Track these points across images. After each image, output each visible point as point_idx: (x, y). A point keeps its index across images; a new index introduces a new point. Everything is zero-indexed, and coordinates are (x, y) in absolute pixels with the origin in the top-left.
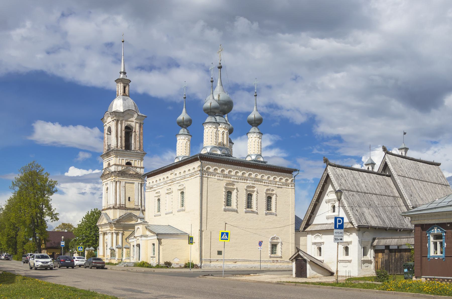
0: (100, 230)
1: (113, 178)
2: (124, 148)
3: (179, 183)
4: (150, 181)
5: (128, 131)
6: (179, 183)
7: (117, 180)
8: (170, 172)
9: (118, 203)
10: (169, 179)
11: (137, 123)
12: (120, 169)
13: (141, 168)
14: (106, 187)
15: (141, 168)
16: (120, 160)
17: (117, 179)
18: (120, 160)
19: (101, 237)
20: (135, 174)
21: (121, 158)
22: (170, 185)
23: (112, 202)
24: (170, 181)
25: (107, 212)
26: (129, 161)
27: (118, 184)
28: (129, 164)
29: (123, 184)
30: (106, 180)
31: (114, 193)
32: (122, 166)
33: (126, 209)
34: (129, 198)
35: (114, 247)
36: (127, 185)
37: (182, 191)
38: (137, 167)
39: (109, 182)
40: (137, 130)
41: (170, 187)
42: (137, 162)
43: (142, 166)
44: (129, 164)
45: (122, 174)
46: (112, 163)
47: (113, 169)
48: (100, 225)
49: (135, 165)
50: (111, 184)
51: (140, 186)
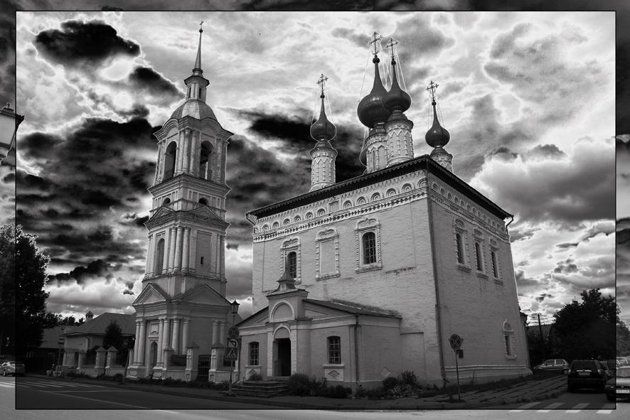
3: (358, 218)
6: (358, 218)
8: (331, 200)
9: (184, 265)
12: (190, 207)
14: (159, 238)
21: (192, 191)
24: (329, 217)
26: (204, 197)
29: (194, 233)
32: (194, 203)
33: (195, 277)
34: (202, 258)
37: (367, 231)
38: (215, 209)
44: (203, 201)
46: (175, 198)
47: (177, 207)
51: (219, 240)
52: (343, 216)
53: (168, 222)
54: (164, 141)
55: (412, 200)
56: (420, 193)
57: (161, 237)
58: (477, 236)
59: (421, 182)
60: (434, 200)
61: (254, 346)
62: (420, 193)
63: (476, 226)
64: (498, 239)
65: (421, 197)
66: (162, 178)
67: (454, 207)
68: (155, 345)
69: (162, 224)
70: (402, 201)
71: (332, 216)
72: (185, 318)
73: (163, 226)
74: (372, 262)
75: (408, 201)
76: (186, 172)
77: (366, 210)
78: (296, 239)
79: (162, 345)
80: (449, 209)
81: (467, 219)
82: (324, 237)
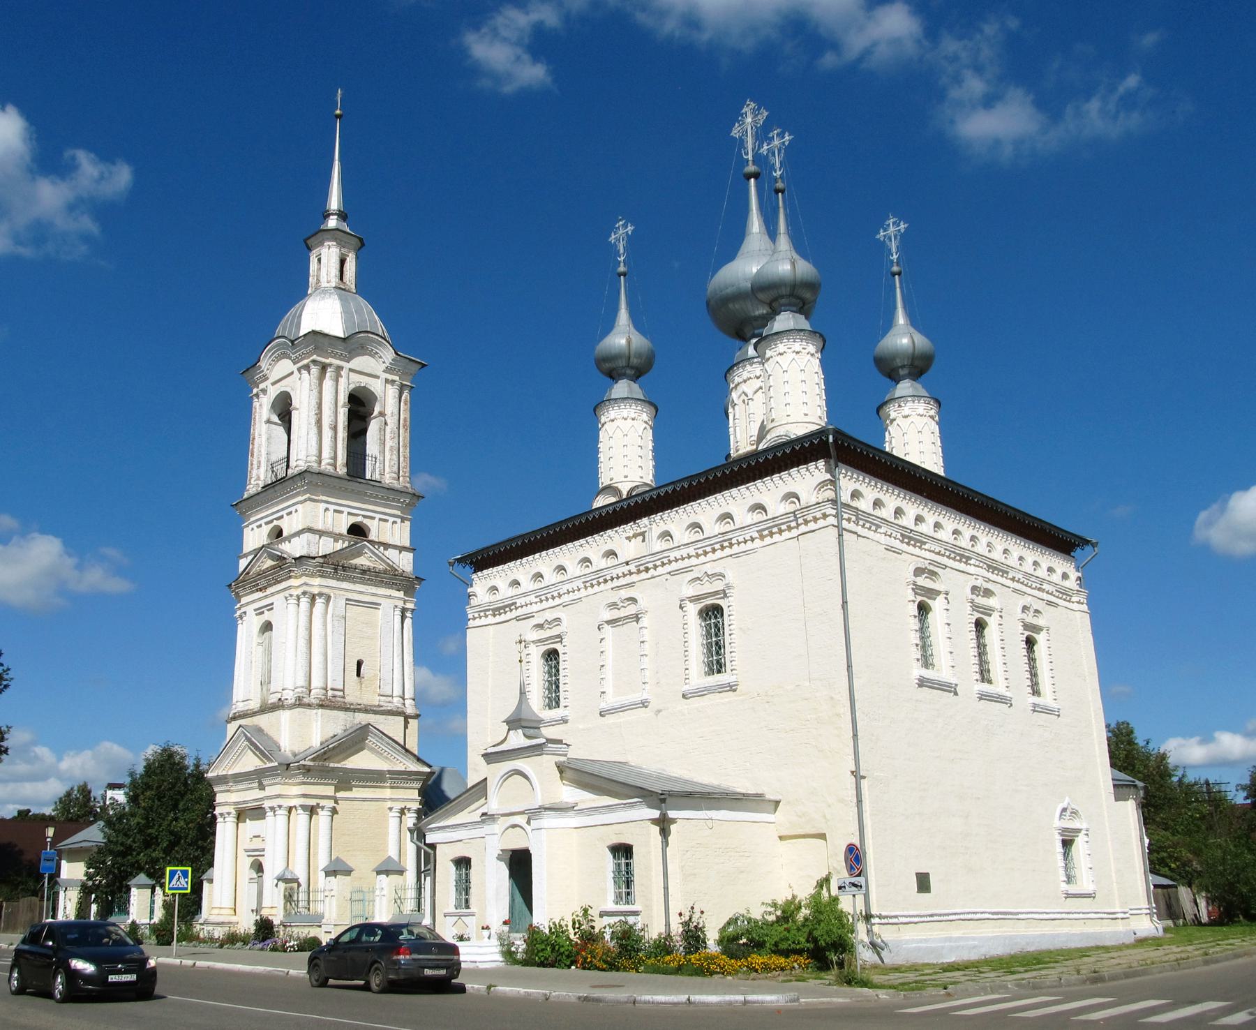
0: (220, 798)
1: (295, 583)
2: (342, 471)
3: (687, 570)
4: (488, 586)
5: (360, 408)
6: (687, 570)
7: (316, 591)
8: (628, 529)
9: (317, 682)
10: (622, 559)
11: (393, 382)
12: (327, 546)
13: (402, 549)
15: (402, 549)
16: (330, 513)
17: (316, 584)
18: (330, 513)
19: (225, 832)
20: (385, 572)
21: (332, 507)
22: (632, 584)
23: (288, 680)
24: (625, 569)
25: (263, 721)
26: (359, 519)
27: (320, 602)
28: (357, 531)
29: (338, 604)
30: (259, 594)
31: (302, 643)
32: (337, 537)
33: (346, 708)
34: (359, 664)
35: (300, 871)
36: (353, 611)
37: (709, 601)
38: (387, 546)
39: (278, 600)
40: (388, 411)
41: (625, 593)
42: (389, 524)
43: (407, 544)
44: (357, 531)
45: (335, 566)
46: (288, 526)
47: (294, 548)
48: (223, 780)
49: (382, 540)
50: (292, 608)
51: (398, 618)
52: (655, 567)
53: (279, 582)
54: (264, 391)
55: (803, 529)
56: (819, 515)
57: (267, 616)
58: (981, 600)
59: (822, 484)
60: (852, 526)
61: (463, 863)
62: (819, 515)
63: (978, 574)
64: (1049, 603)
65: (821, 523)
66: (262, 477)
67: (909, 537)
68: (259, 868)
69: (266, 588)
70: (781, 532)
71: (632, 568)
72: (322, 802)
73: (270, 590)
74: (719, 672)
75: (795, 533)
76: (315, 465)
77: (706, 553)
78: (558, 619)
79: (273, 867)
80: (897, 544)
81: (950, 563)
82: (616, 614)
